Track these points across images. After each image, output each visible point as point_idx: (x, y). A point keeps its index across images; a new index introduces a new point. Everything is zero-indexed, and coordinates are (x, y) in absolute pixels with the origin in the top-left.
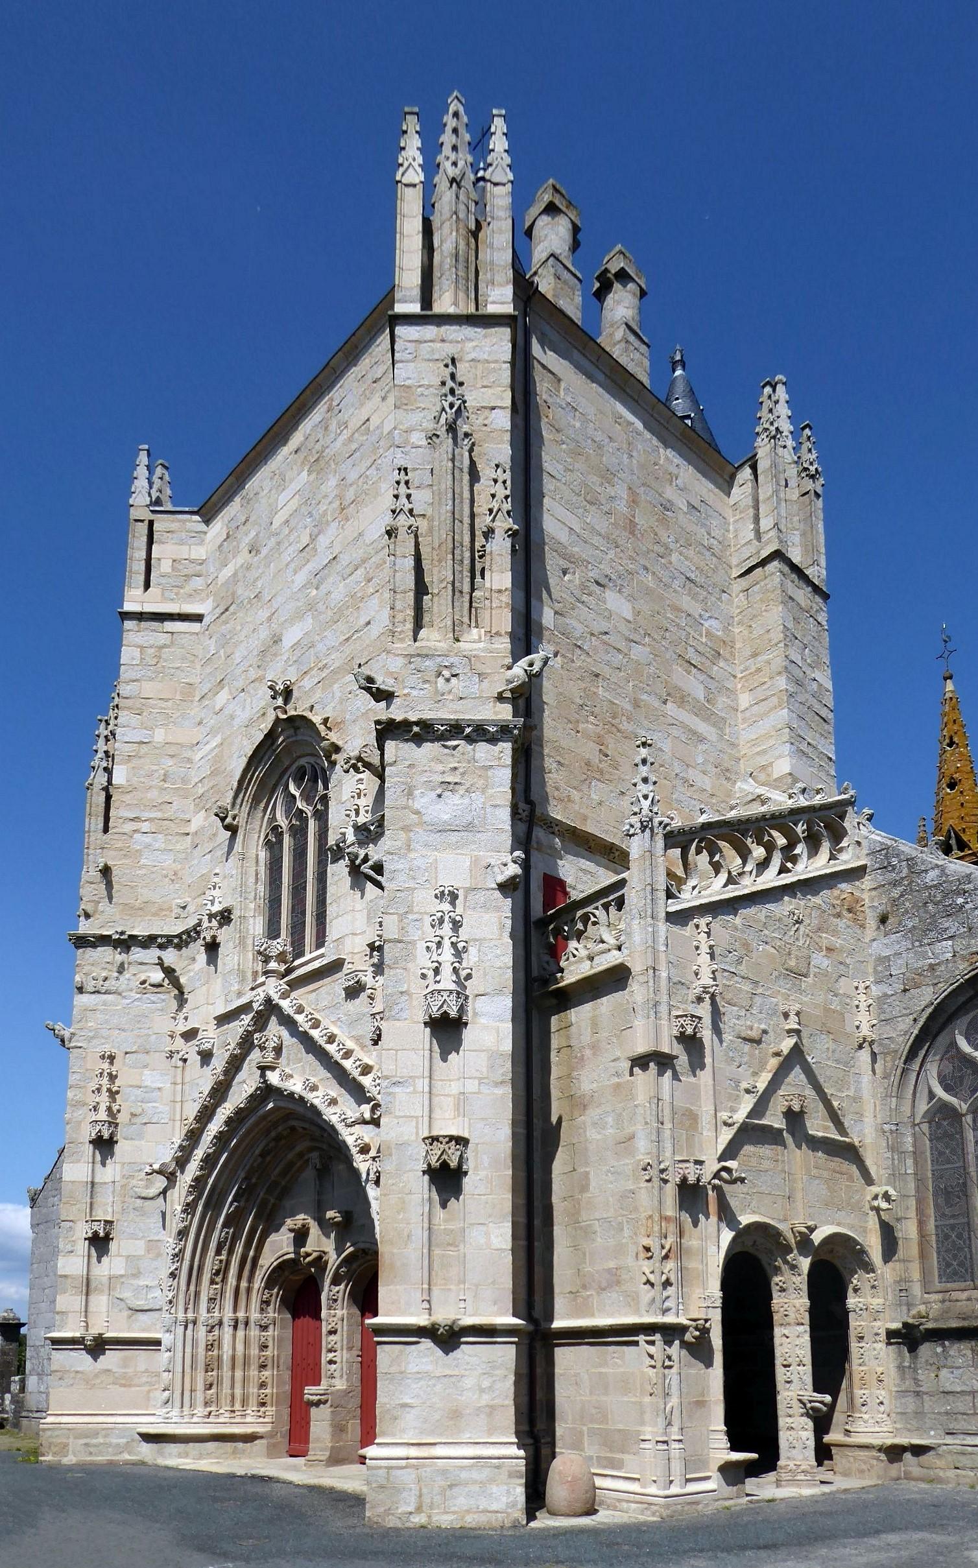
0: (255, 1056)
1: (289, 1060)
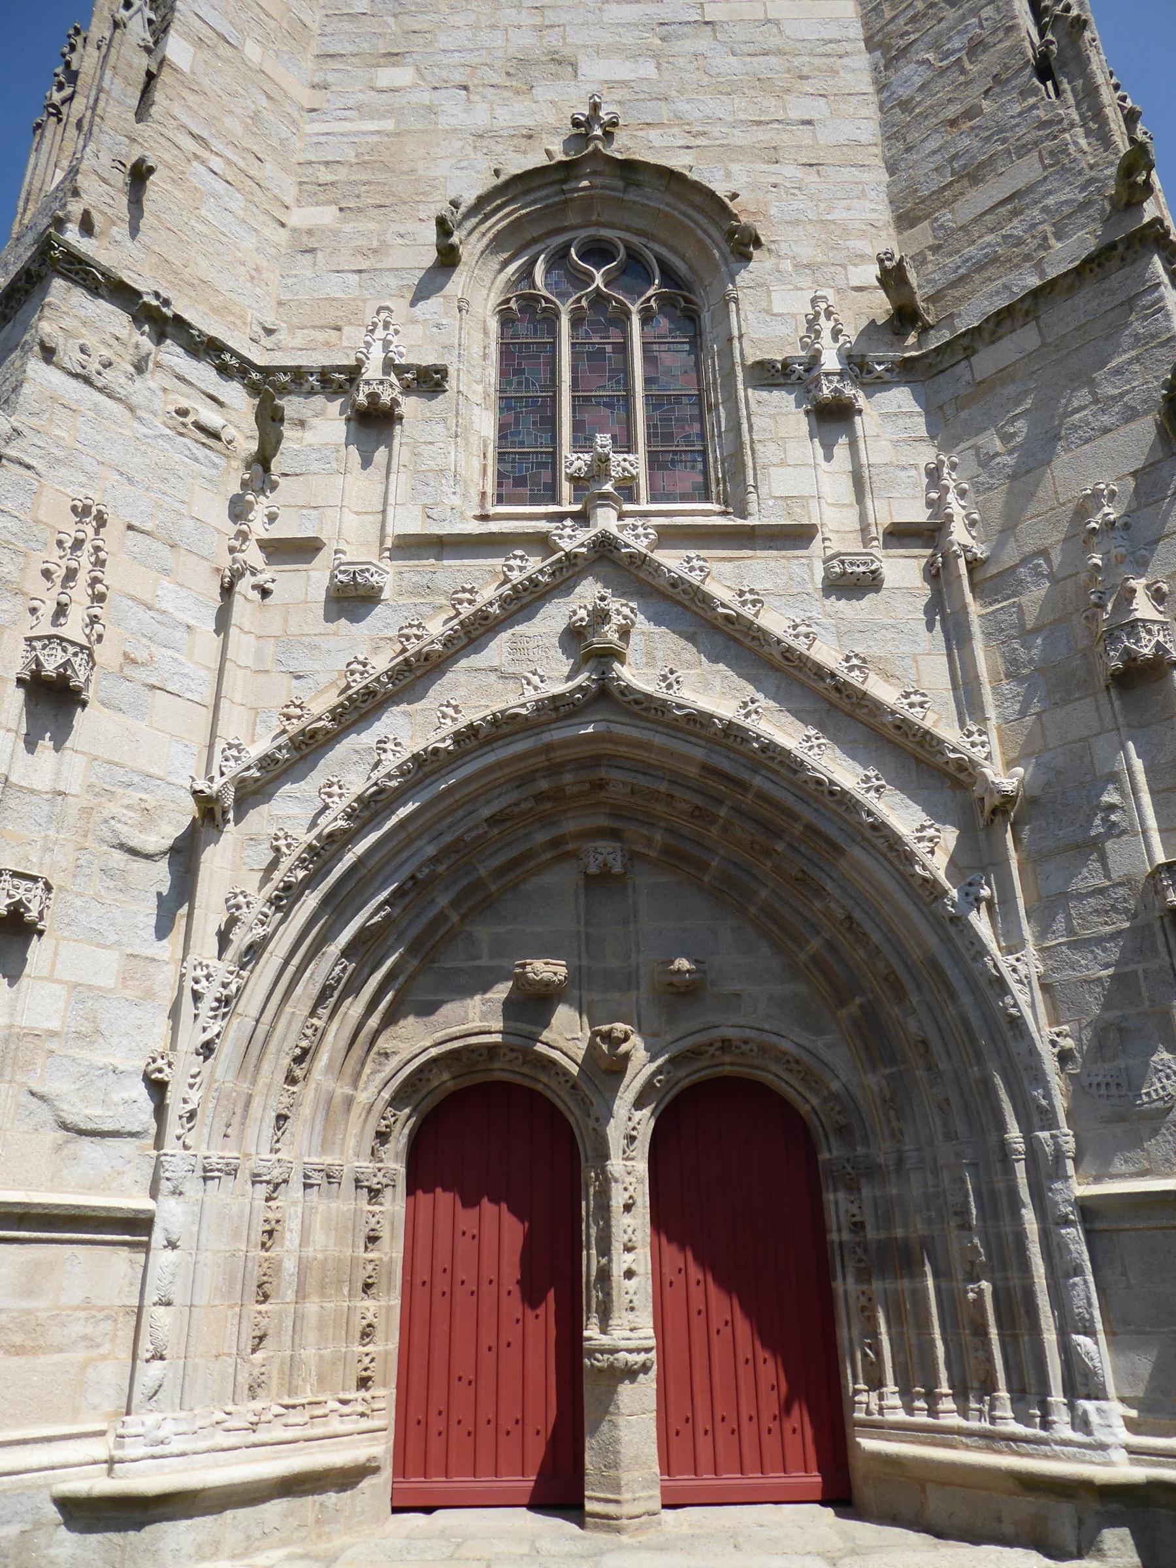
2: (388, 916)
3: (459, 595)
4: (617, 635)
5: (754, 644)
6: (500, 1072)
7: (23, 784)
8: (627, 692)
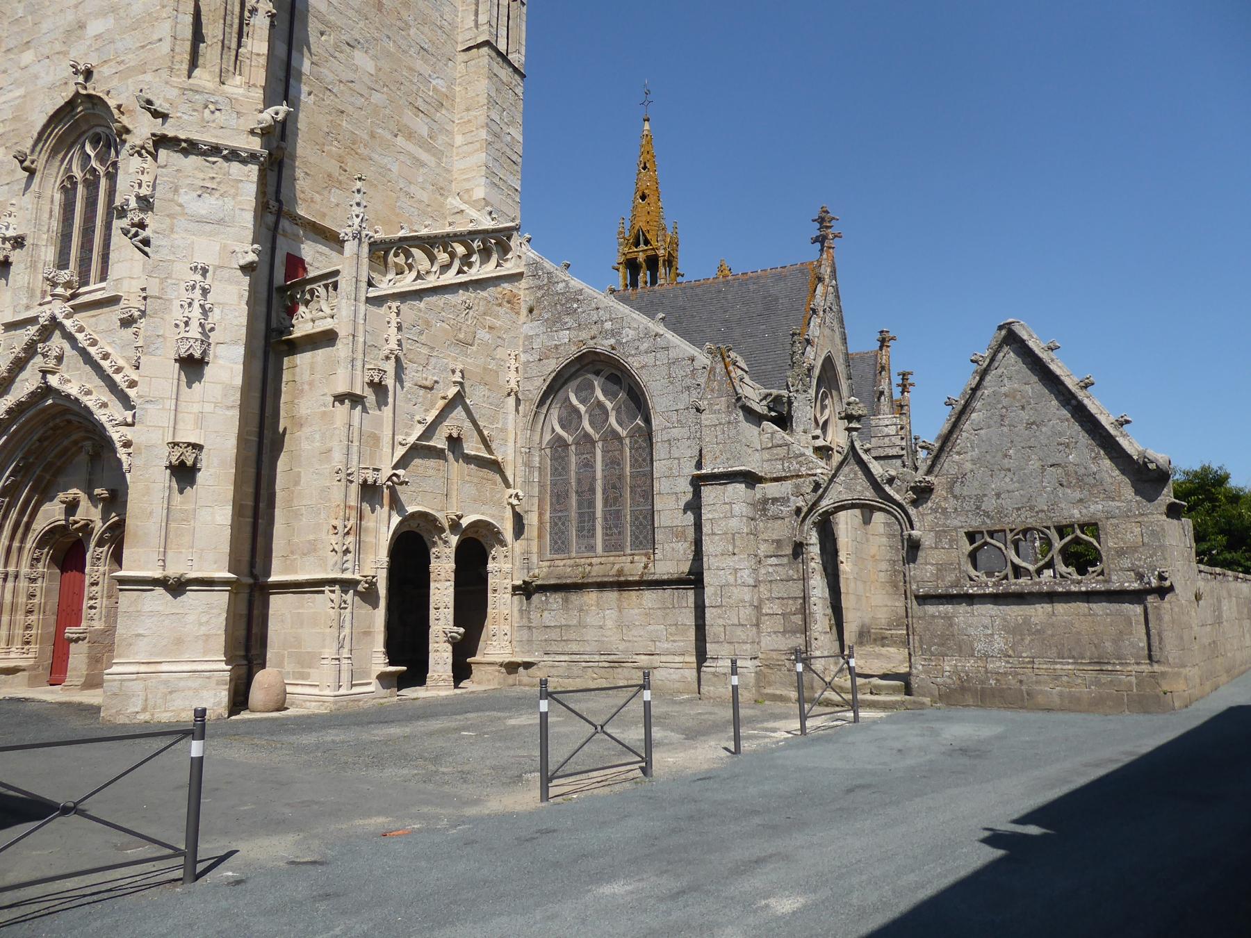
0: (38, 361)
1: (68, 367)
2: (13, 481)
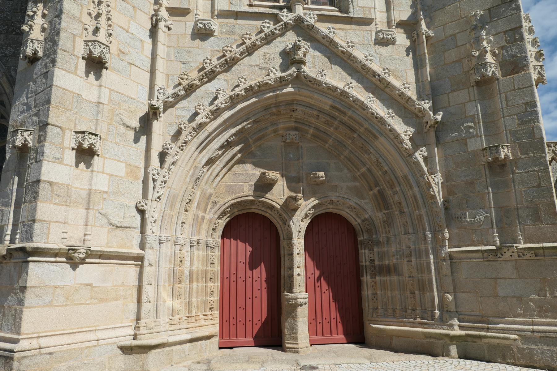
3: (245, 36)
4: (303, 56)
5: (351, 62)
6: (254, 209)
7: (87, 99)
8: (306, 77)
